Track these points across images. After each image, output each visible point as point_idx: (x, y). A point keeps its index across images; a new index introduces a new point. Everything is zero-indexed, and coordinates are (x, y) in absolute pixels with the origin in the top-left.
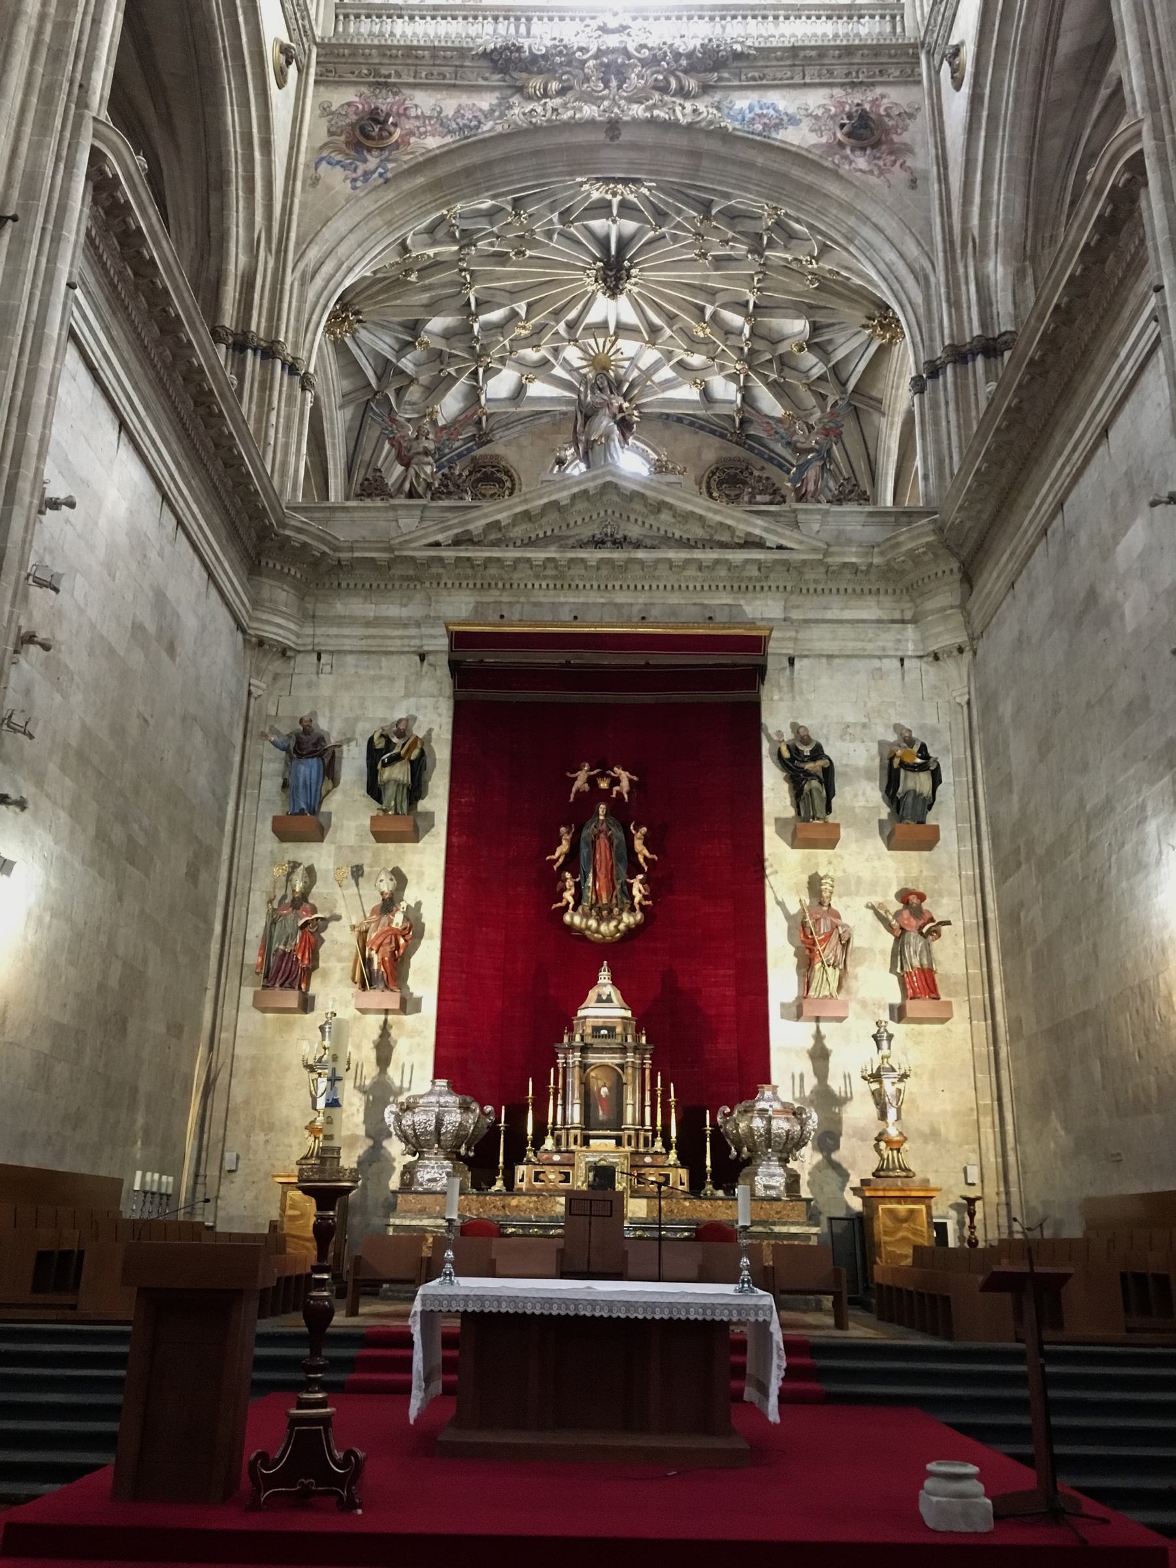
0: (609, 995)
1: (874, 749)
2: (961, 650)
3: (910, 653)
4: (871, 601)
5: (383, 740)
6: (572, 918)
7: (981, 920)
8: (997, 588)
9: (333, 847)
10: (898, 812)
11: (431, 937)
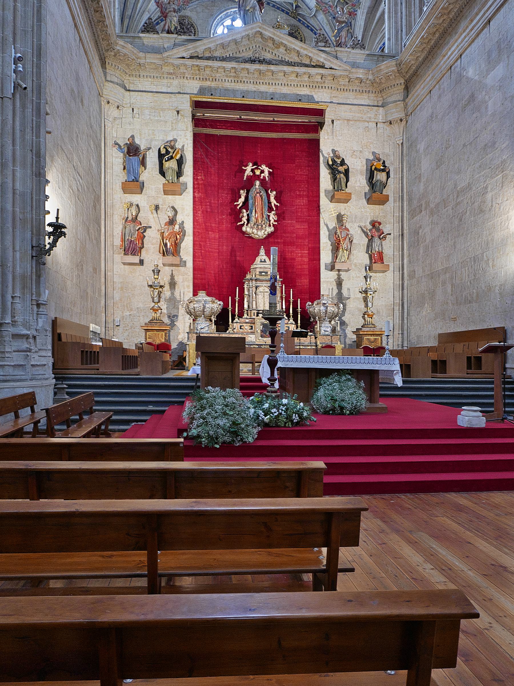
0: (265, 260)
1: (365, 161)
2: (401, 120)
3: (380, 121)
4: (365, 96)
5: (165, 149)
6: (246, 228)
7: (401, 233)
8: (422, 93)
9: (146, 196)
10: (373, 189)
11: (189, 236)
